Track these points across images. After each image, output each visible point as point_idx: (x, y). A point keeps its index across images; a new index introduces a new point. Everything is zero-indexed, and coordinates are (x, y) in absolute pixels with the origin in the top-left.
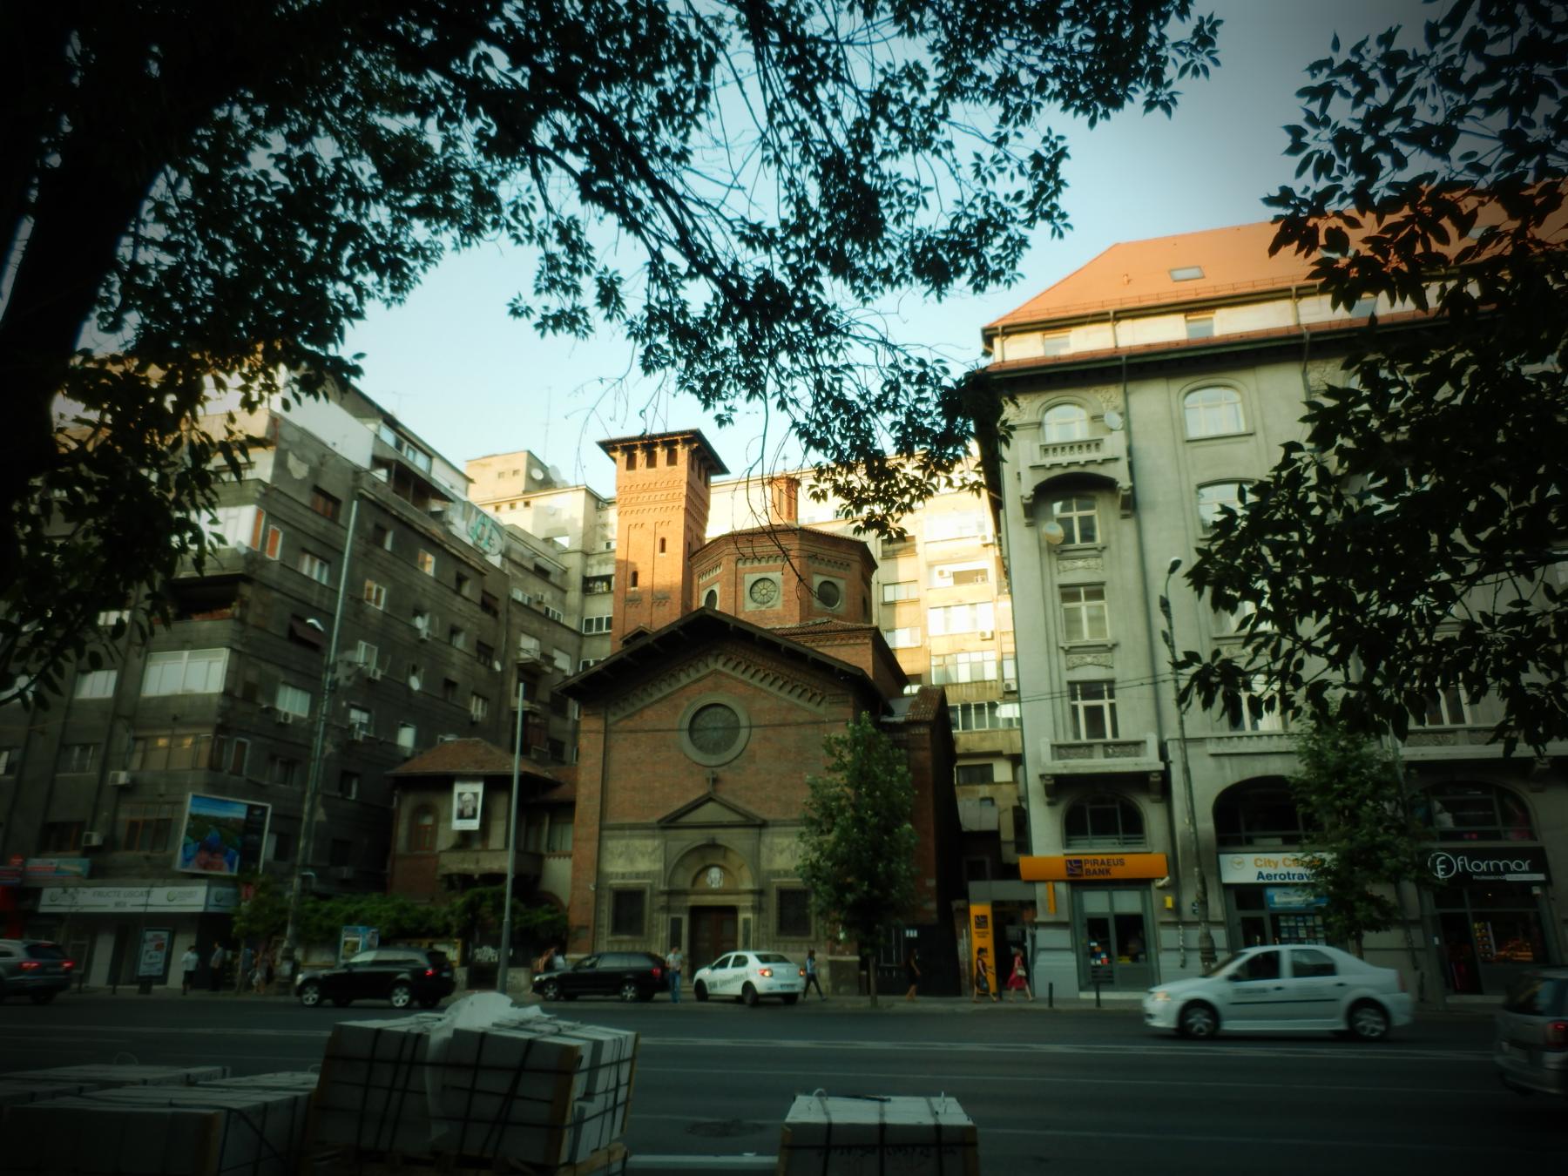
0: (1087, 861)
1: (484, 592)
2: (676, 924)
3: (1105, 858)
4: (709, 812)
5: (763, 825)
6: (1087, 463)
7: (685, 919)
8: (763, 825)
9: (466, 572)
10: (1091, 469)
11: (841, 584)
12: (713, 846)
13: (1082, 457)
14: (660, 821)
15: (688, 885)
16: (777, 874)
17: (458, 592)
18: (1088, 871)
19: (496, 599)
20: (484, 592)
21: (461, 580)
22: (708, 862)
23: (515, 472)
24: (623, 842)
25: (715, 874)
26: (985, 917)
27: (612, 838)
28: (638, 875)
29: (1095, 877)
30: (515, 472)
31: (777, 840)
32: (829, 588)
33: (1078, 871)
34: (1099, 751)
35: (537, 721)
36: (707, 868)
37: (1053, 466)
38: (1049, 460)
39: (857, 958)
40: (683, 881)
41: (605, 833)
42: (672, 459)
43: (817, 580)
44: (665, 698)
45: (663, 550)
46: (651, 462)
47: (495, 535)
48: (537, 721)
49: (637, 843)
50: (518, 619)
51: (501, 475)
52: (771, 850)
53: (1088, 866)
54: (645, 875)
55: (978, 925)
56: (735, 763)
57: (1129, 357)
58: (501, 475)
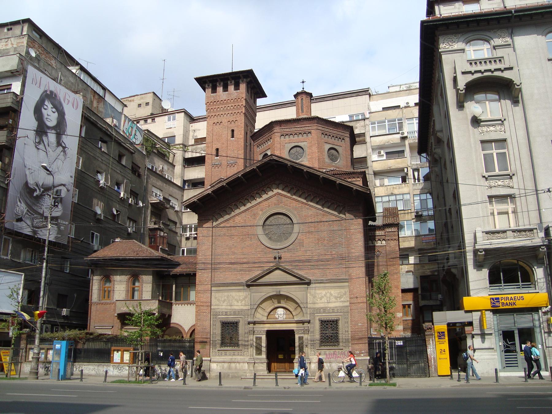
0: (502, 298)
1: (133, 162)
5: (309, 284)
6: (496, 70)
7: (264, 337)
9: (123, 151)
10: (497, 74)
11: (340, 149)
13: (493, 67)
14: (247, 281)
15: (265, 319)
16: (318, 310)
17: (119, 161)
18: (503, 303)
19: (140, 168)
20: (133, 162)
21: (121, 156)
23: (147, 104)
24: (226, 294)
26: (444, 332)
28: (235, 313)
29: (507, 307)
30: (147, 104)
31: (318, 292)
33: (497, 304)
34: (509, 233)
35: (162, 234)
37: (476, 72)
38: (474, 68)
39: (369, 358)
40: (261, 315)
42: (237, 87)
43: (328, 147)
44: (248, 209)
45: (233, 137)
46: (225, 89)
47: (138, 133)
48: (162, 234)
49: (234, 294)
50: (153, 180)
51: (140, 105)
52: (314, 297)
53: (503, 301)
54: (240, 312)
55: (440, 337)
56: (290, 247)
57: (516, 12)
58: (140, 105)
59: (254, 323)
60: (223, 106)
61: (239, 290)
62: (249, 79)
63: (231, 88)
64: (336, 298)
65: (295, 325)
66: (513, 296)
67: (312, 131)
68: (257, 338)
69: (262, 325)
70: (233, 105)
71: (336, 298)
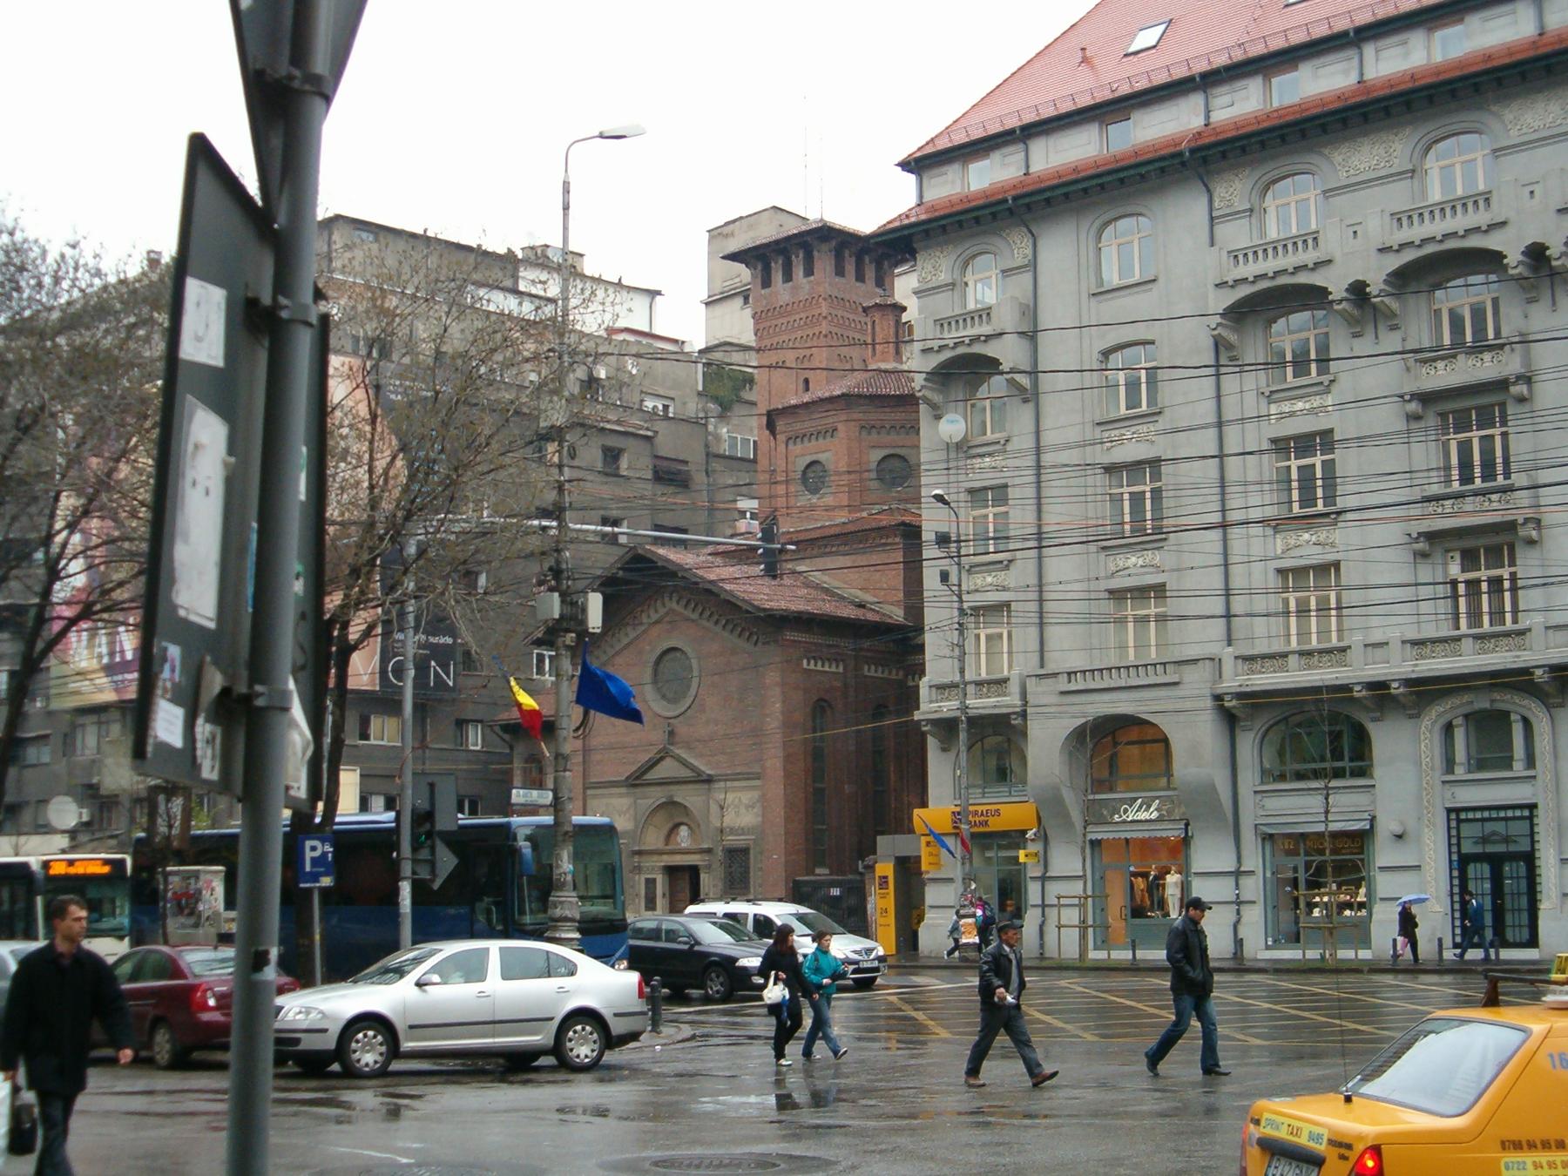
2: (651, 883)
3: (985, 808)
4: (667, 769)
8: (709, 780)
12: (671, 804)
15: (660, 845)
19: (685, 462)
22: (678, 820)
24: (604, 801)
25: (684, 831)
27: (595, 796)
32: (897, 463)
36: (677, 825)
40: (653, 839)
41: (589, 792)
43: (876, 455)
57: (1015, 199)
59: (640, 853)
60: (784, 320)
61: (621, 795)
62: (834, 243)
63: (799, 271)
64: (747, 807)
65: (697, 857)
66: (985, 808)
67: (840, 427)
68: (647, 880)
69: (655, 858)
70: (803, 315)
71: (747, 807)
